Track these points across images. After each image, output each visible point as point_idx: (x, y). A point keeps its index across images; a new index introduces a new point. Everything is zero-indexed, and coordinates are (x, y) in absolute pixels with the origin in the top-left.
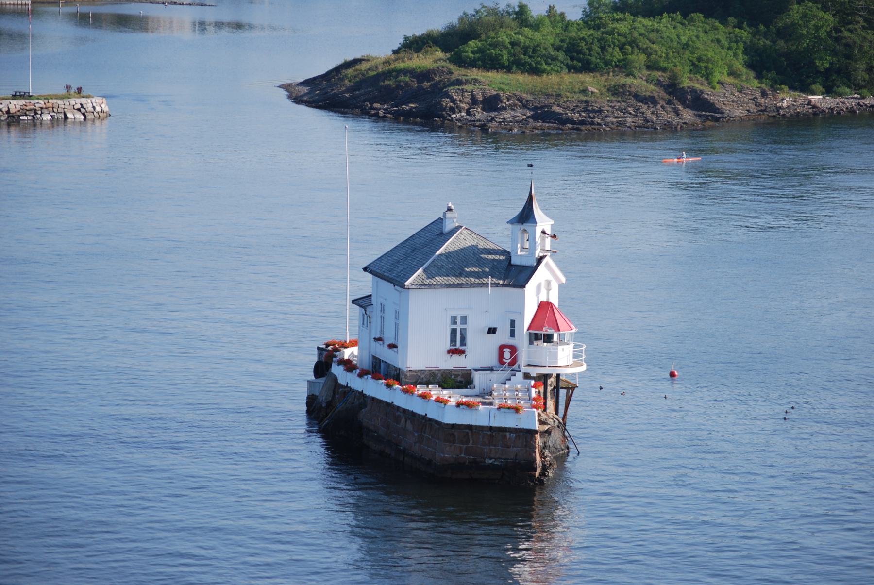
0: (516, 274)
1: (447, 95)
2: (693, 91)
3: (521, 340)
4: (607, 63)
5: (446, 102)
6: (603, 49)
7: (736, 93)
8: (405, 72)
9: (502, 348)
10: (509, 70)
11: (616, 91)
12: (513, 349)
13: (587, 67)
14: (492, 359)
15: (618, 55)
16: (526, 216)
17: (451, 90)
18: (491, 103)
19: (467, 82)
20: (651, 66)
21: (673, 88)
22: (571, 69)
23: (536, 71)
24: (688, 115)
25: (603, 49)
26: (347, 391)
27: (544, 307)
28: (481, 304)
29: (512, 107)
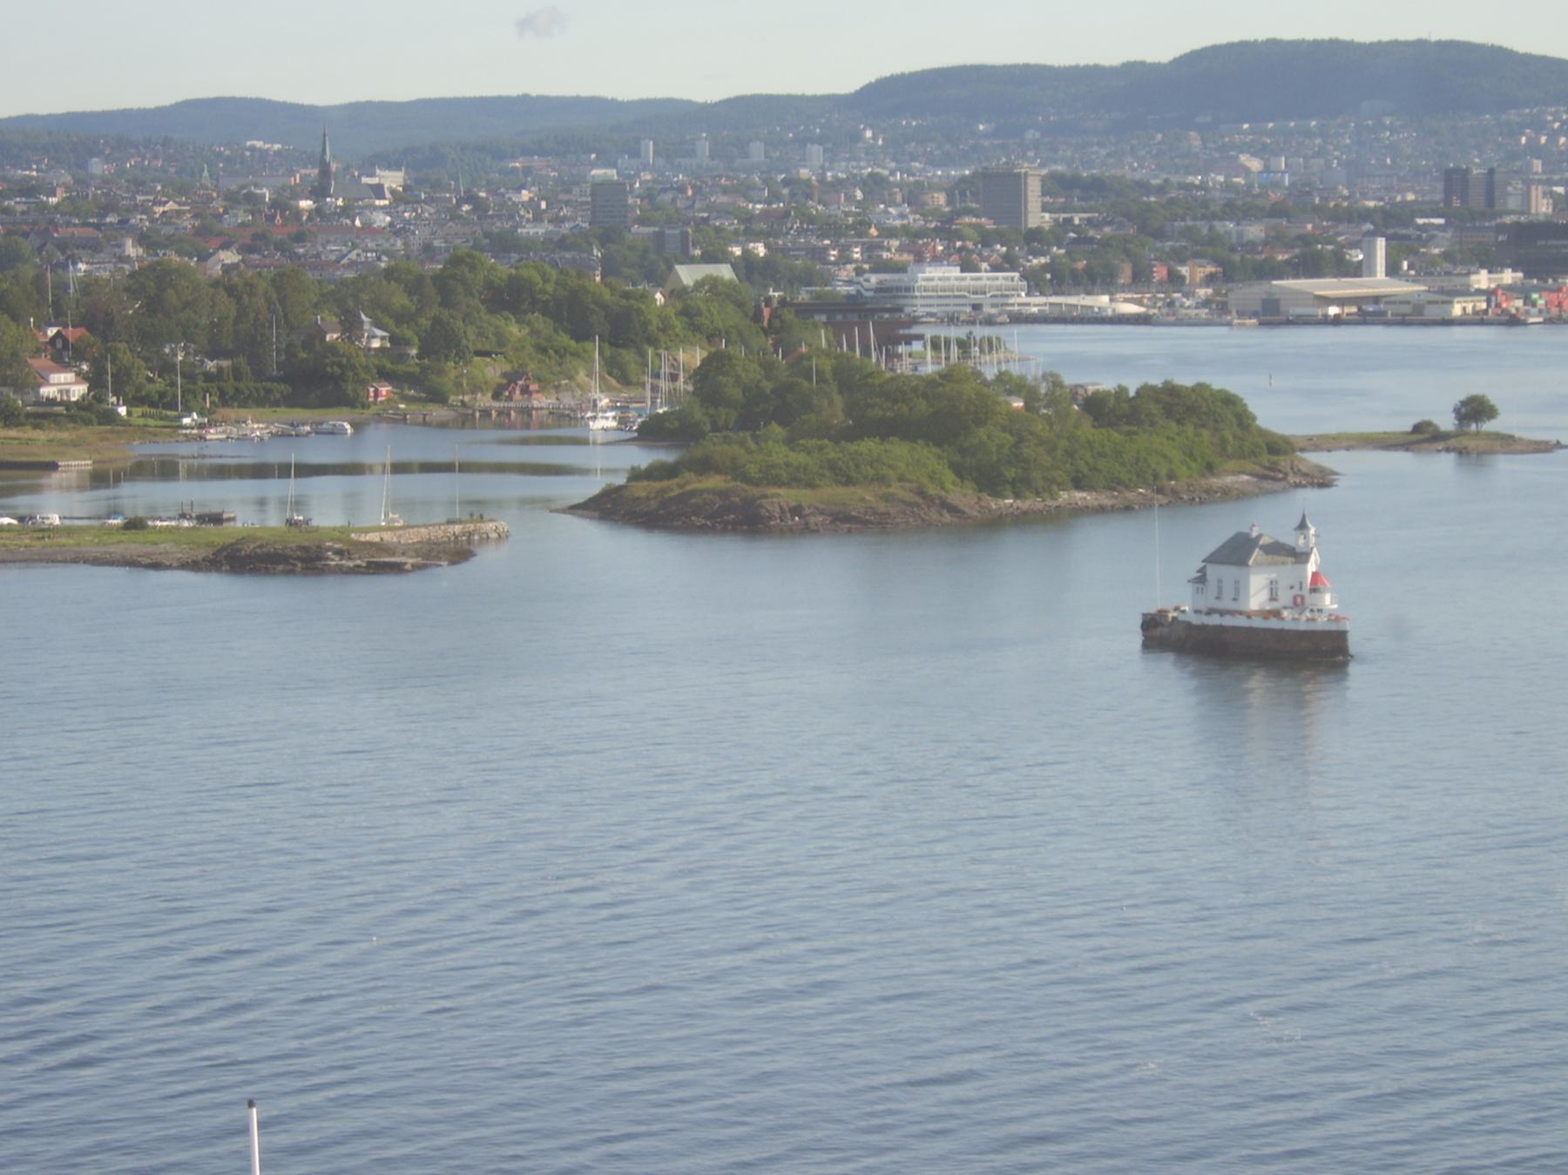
0: (1301, 557)
1: (761, 506)
2: (940, 498)
3: (1305, 592)
4: (865, 478)
5: (763, 512)
6: (857, 466)
7: (964, 496)
8: (708, 491)
9: (1295, 597)
10: (788, 485)
11: (888, 498)
12: (1303, 598)
13: (848, 481)
14: (1289, 602)
15: (871, 472)
16: (1302, 526)
17: (764, 501)
18: (797, 510)
19: (773, 496)
20: (901, 479)
21: (921, 493)
22: (838, 482)
23: (811, 485)
24: (947, 517)
25: (857, 466)
26: (1203, 628)
27: (1315, 575)
28: (1285, 573)
29: (812, 514)
